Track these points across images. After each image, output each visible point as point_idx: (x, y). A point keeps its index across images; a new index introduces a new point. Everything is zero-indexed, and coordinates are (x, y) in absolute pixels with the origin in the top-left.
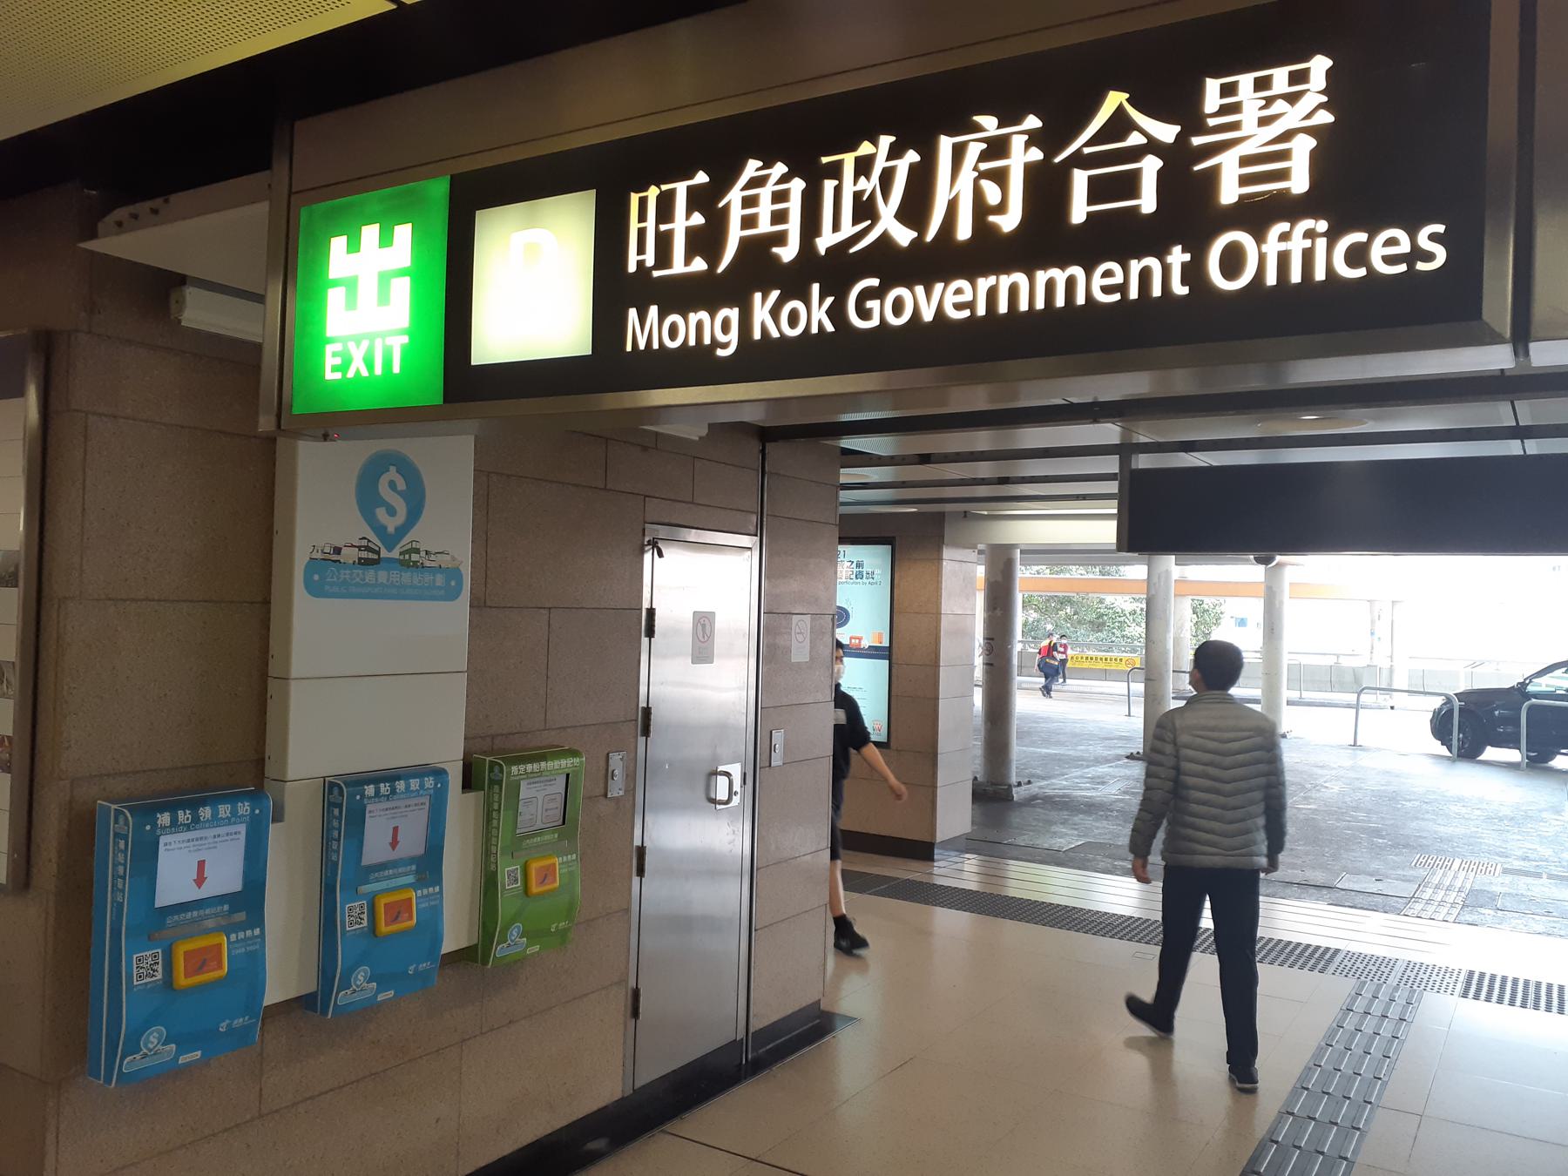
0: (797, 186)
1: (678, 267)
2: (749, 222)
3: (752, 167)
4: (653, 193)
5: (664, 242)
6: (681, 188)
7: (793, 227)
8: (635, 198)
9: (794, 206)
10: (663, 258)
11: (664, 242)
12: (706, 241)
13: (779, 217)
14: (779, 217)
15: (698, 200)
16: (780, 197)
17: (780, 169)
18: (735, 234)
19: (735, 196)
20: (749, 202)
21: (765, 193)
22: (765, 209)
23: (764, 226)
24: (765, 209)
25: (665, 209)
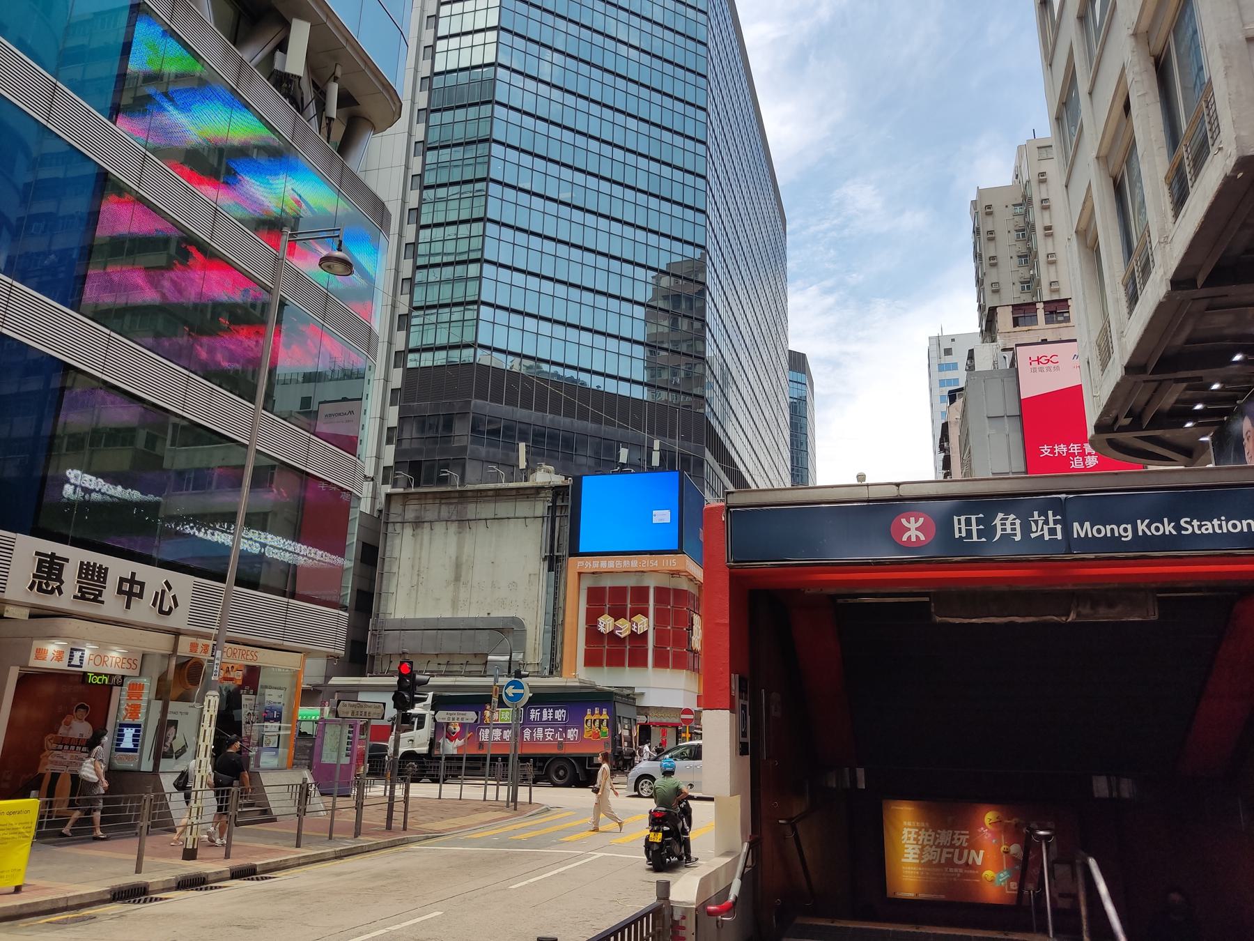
0: (1018, 522)
1: (975, 539)
3: (1000, 515)
4: (963, 518)
5: (969, 533)
6: (973, 518)
7: (1018, 532)
8: (956, 518)
9: (1018, 527)
11: (969, 533)
13: (1014, 529)
14: (1014, 529)
15: (979, 522)
17: (1012, 516)
19: (997, 522)
21: (1008, 523)
22: (1008, 527)
23: (1009, 531)
24: (1008, 527)
25: (968, 522)
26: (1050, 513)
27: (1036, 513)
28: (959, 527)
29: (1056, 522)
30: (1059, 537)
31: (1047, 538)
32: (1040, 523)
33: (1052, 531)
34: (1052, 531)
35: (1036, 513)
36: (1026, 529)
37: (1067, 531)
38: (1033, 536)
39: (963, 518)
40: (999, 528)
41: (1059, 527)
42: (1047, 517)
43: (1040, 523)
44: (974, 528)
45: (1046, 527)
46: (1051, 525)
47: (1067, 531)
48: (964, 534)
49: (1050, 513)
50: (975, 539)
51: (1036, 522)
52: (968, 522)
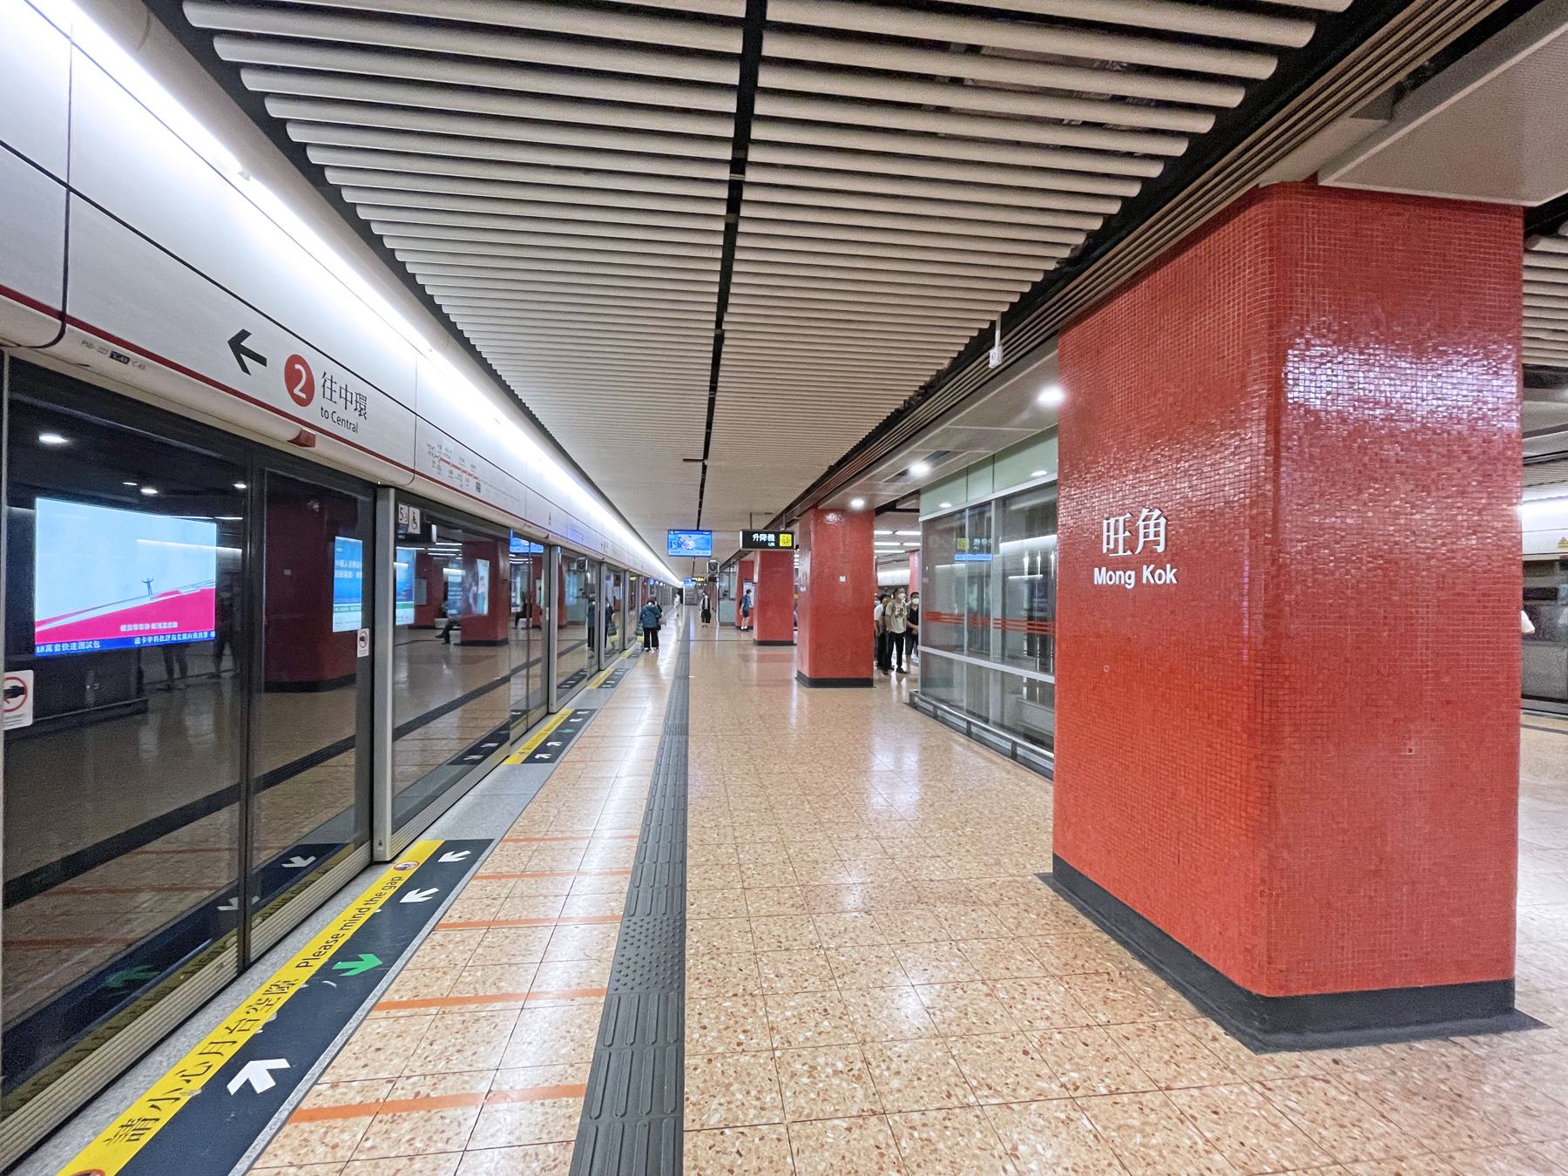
0: (1163, 521)
1: (1121, 553)
4: (1112, 521)
5: (1116, 541)
6: (1121, 519)
7: (1162, 539)
9: (1162, 529)
10: (1115, 550)
11: (1116, 541)
12: (1130, 544)
13: (1157, 534)
14: (1157, 534)
16: (1157, 525)
17: (1157, 513)
18: (1142, 540)
20: (1146, 527)
21: (1152, 523)
22: (1152, 530)
23: (1152, 538)
24: (1152, 530)
39: (1112, 521)
40: (1142, 531)
44: (1121, 536)
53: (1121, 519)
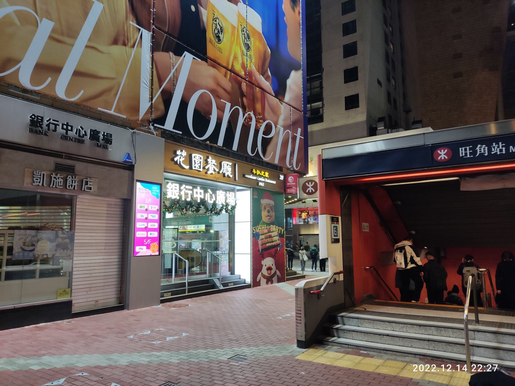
0: (486, 148)
1: (468, 156)
2: (480, 151)
3: (479, 146)
4: (463, 148)
5: (466, 154)
6: (468, 148)
7: (486, 152)
8: (460, 149)
9: (486, 150)
11: (466, 154)
13: (484, 151)
14: (484, 151)
15: (470, 149)
16: (484, 149)
17: (484, 146)
19: (478, 148)
20: (480, 149)
21: (482, 148)
23: (482, 152)
25: (466, 150)
26: (500, 143)
27: (494, 144)
28: (462, 152)
29: (503, 147)
30: (504, 152)
31: (498, 153)
32: (496, 147)
33: (501, 150)
34: (501, 150)
35: (494, 144)
36: (490, 150)
37: (507, 149)
38: (493, 153)
39: (463, 148)
40: (478, 151)
41: (504, 148)
42: (499, 144)
43: (496, 147)
44: (468, 152)
45: (498, 149)
46: (501, 148)
47: (507, 149)
48: (464, 155)
49: (500, 143)
50: (468, 156)
51: (494, 147)
52: (466, 150)
53: (468, 148)
